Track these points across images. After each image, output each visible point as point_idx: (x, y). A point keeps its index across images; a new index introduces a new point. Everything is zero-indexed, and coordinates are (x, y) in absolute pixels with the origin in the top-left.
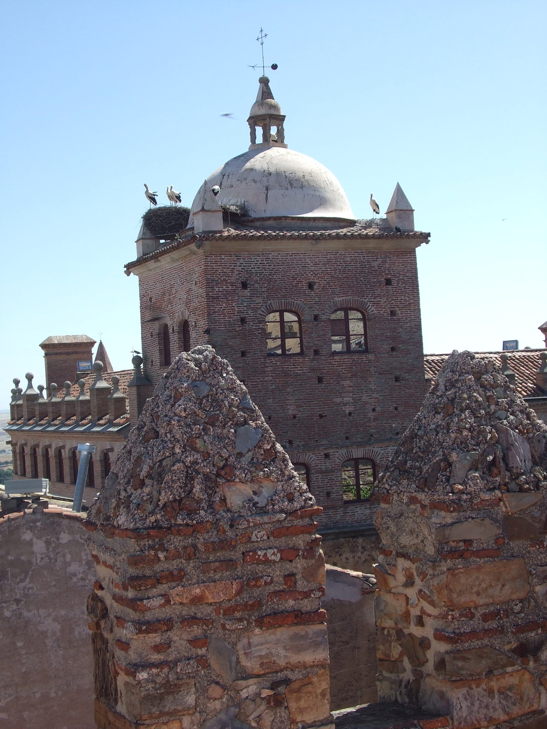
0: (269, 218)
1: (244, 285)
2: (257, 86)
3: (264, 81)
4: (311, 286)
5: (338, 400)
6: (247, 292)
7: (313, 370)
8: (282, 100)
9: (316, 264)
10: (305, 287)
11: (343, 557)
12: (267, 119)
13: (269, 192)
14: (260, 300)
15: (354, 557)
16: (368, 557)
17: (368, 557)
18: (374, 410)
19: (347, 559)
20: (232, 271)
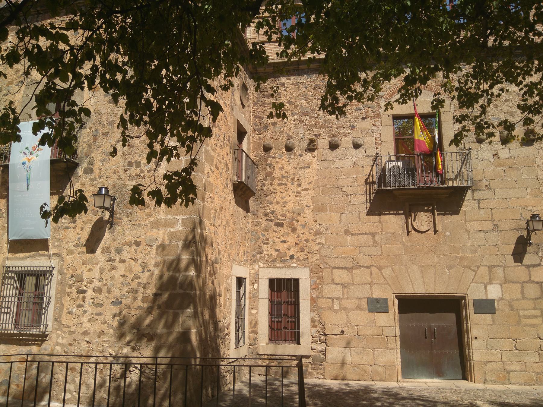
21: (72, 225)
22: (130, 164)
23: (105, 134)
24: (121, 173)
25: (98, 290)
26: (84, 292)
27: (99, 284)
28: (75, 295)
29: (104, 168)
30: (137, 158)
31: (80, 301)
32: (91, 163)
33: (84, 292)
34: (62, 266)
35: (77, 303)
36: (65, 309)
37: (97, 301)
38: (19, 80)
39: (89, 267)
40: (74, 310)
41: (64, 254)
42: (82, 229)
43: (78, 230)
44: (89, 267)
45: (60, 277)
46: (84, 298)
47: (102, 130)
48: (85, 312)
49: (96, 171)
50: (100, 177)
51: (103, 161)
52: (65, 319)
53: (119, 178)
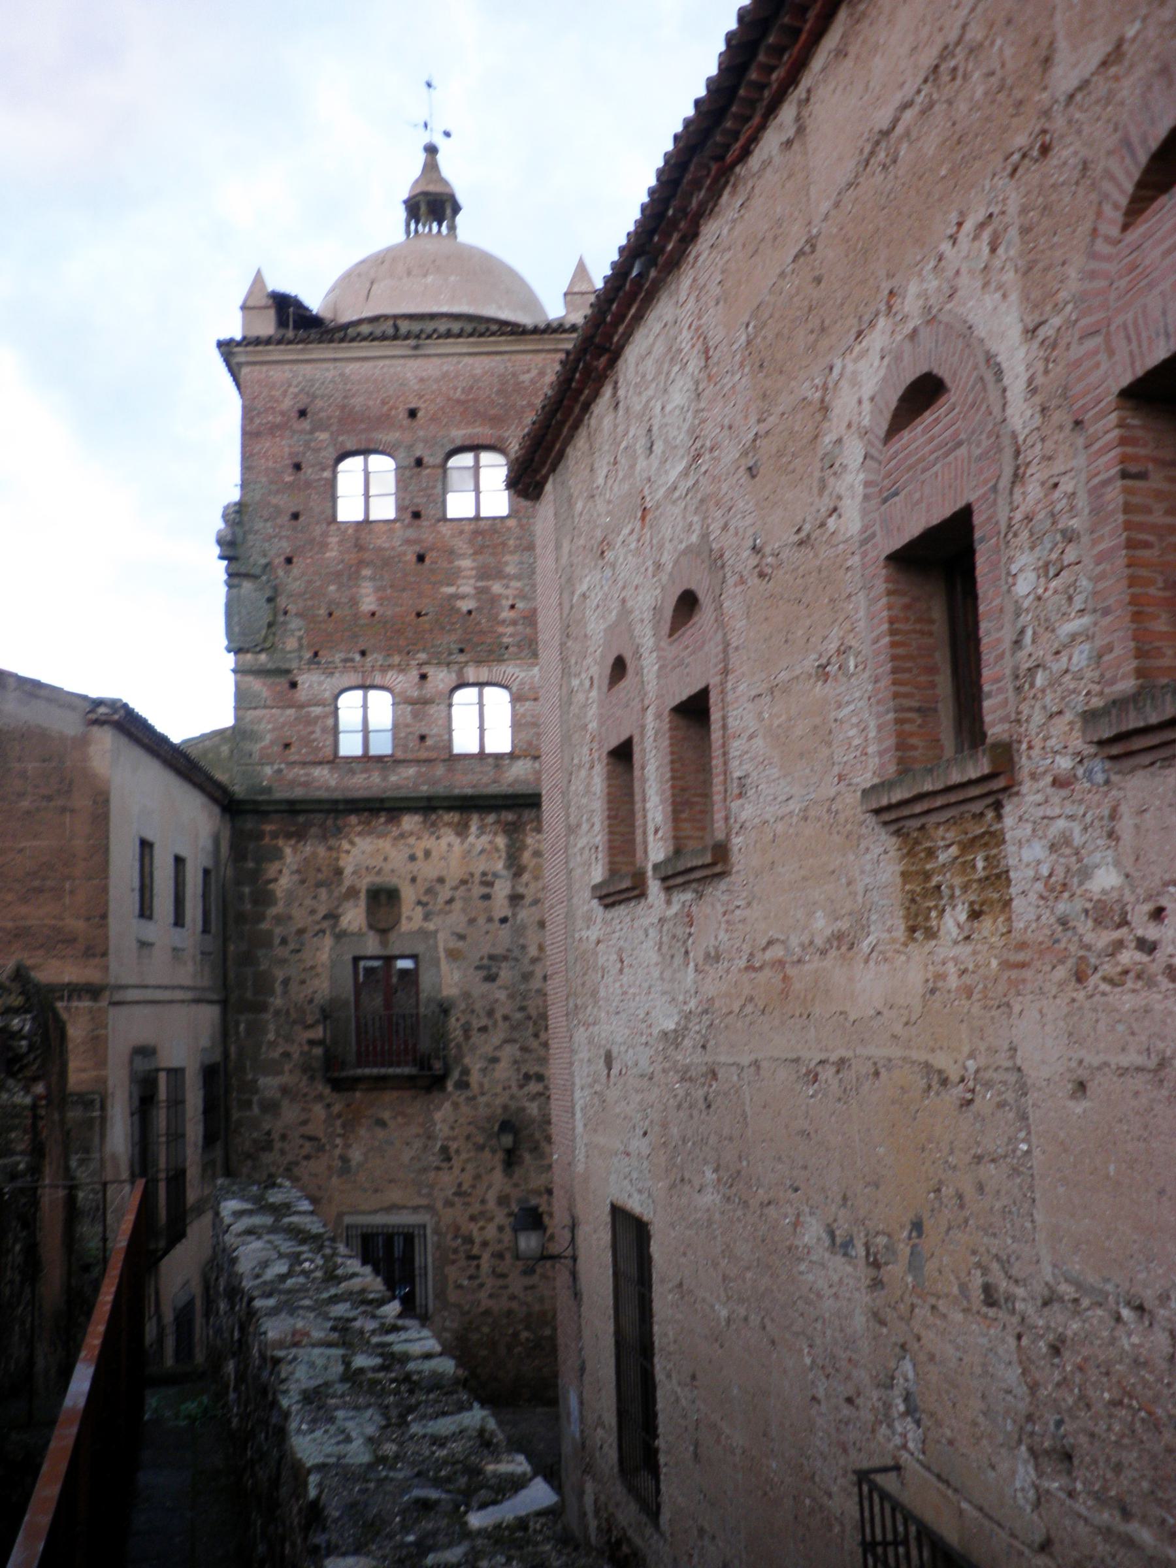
0: (360, 322)
1: (303, 413)
2: (421, 157)
3: (431, 150)
4: (413, 414)
5: (451, 590)
6: (306, 424)
7: (408, 542)
8: (456, 173)
9: (422, 380)
10: (402, 415)
11: (444, 842)
12: (432, 205)
13: (375, 287)
14: (323, 436)
15: (462, 843)
16: (488, 847)
17: (488, 847)
18: (513, 607)
19: (449, 845)
20: (285, 393)
21: (445, 1165)
22: (527, 1077)
23: (483, 1029)
24: (515, 1089)
25: (499, 1256)
26: (477, 1257)
27: (498, 1247)
28: (463, 1263)
29: (486, 1081)
30: (536, 1069)
31: (472, 1271)
32: (466, 1072)
33: (477, 1257)
34: (437, 1223)
35: (469, 1273)
36: (450, 1282)
37: (499, 1270)
38: (317, 927)
39: (481, 1224)
40: (466, 1283)
41: (439, 1205)
42: (463, 1170)
43: (456, 1171)
44: (481, 1224)
45: (436, 1238)
46: (478, 1267)
47: (476, 1024)
48: (481, 1285)
49: (474, 1085)
50: (483, 1094)
51: (484, 1071)
52: (453, 1296)
53: (512, 1097)
